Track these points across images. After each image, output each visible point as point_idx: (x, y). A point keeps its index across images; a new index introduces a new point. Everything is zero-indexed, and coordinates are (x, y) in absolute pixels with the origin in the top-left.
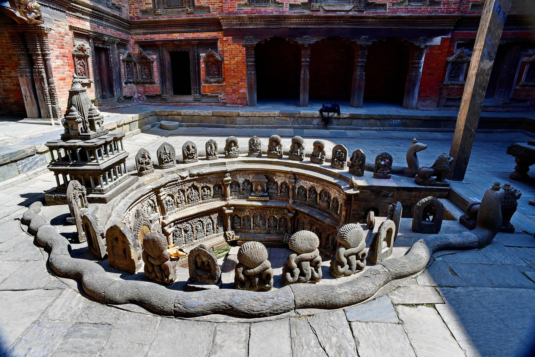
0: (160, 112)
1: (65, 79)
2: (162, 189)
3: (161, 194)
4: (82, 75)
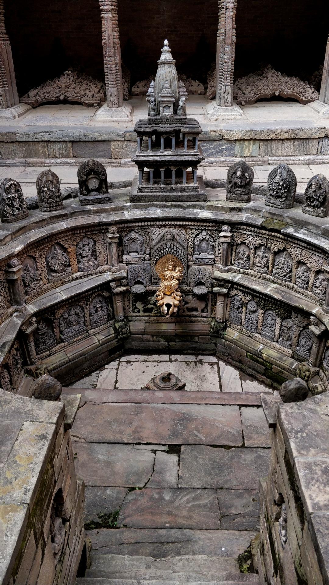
2: (225, 227)
3: (222, 234)
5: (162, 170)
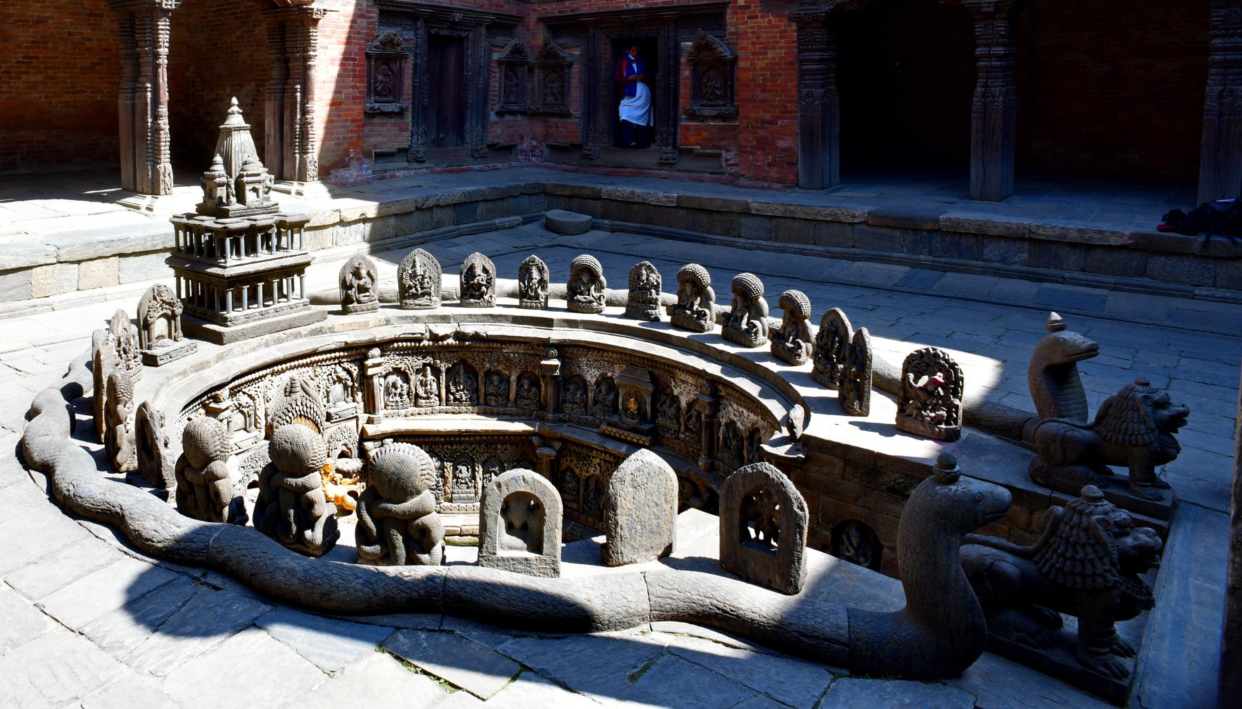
0: (554, 185)
1: (340, 104)
3: (369, 362)
4: (386, 96)
5: (261, 285)
